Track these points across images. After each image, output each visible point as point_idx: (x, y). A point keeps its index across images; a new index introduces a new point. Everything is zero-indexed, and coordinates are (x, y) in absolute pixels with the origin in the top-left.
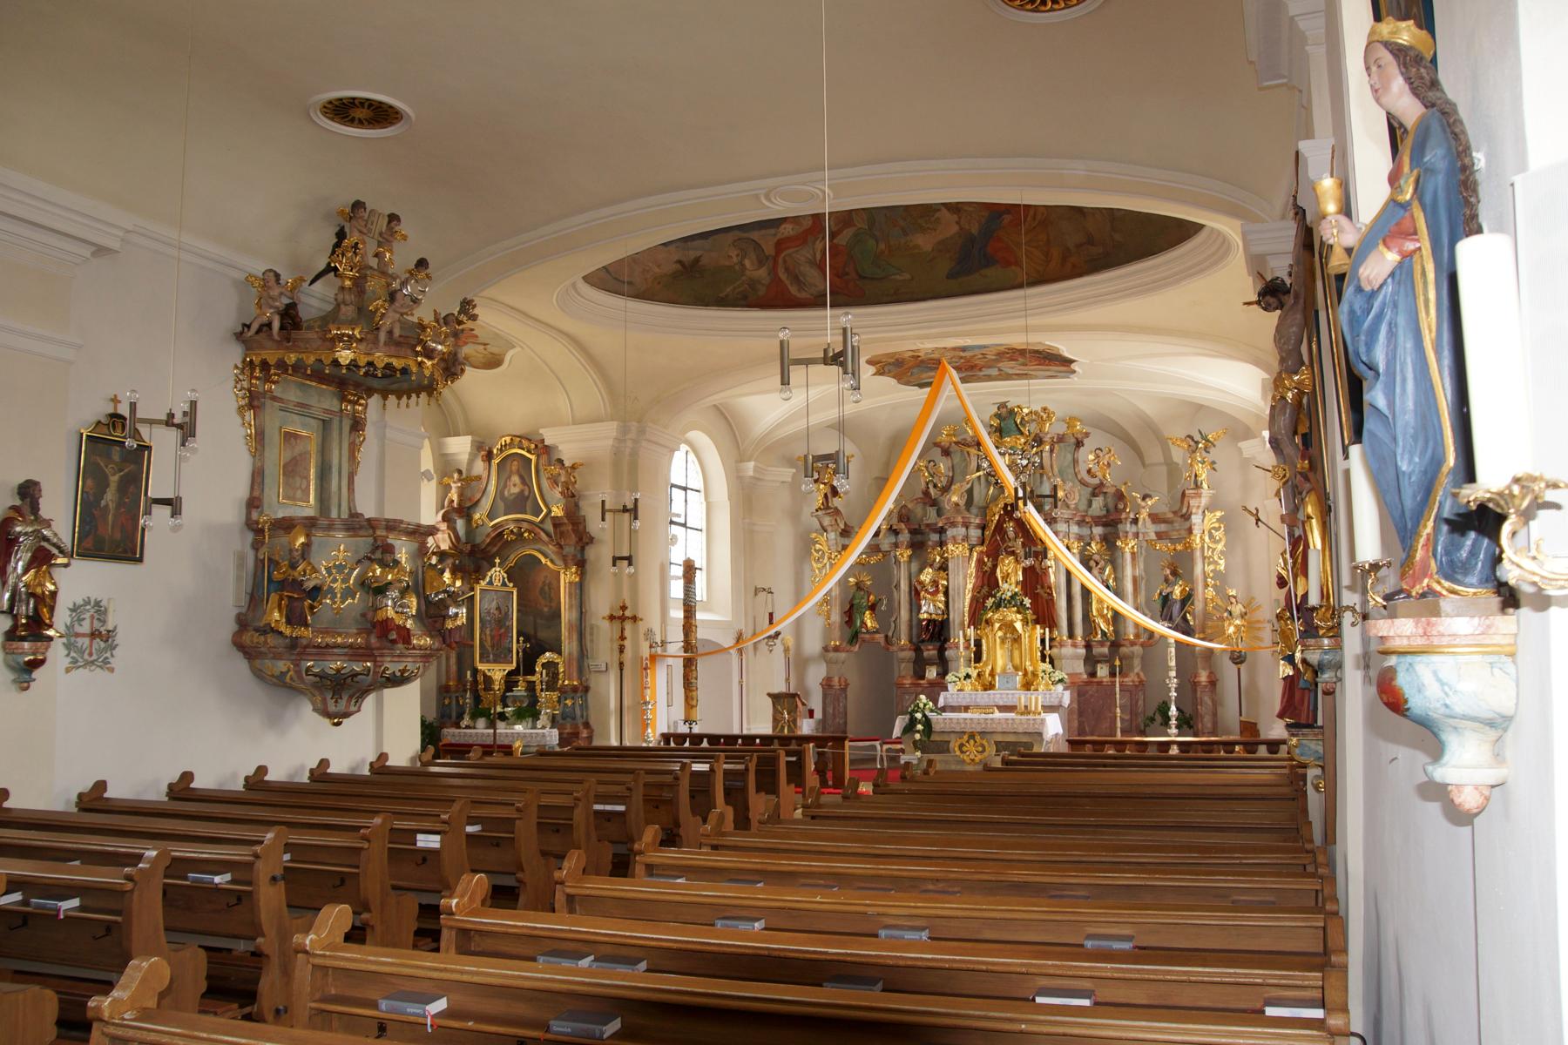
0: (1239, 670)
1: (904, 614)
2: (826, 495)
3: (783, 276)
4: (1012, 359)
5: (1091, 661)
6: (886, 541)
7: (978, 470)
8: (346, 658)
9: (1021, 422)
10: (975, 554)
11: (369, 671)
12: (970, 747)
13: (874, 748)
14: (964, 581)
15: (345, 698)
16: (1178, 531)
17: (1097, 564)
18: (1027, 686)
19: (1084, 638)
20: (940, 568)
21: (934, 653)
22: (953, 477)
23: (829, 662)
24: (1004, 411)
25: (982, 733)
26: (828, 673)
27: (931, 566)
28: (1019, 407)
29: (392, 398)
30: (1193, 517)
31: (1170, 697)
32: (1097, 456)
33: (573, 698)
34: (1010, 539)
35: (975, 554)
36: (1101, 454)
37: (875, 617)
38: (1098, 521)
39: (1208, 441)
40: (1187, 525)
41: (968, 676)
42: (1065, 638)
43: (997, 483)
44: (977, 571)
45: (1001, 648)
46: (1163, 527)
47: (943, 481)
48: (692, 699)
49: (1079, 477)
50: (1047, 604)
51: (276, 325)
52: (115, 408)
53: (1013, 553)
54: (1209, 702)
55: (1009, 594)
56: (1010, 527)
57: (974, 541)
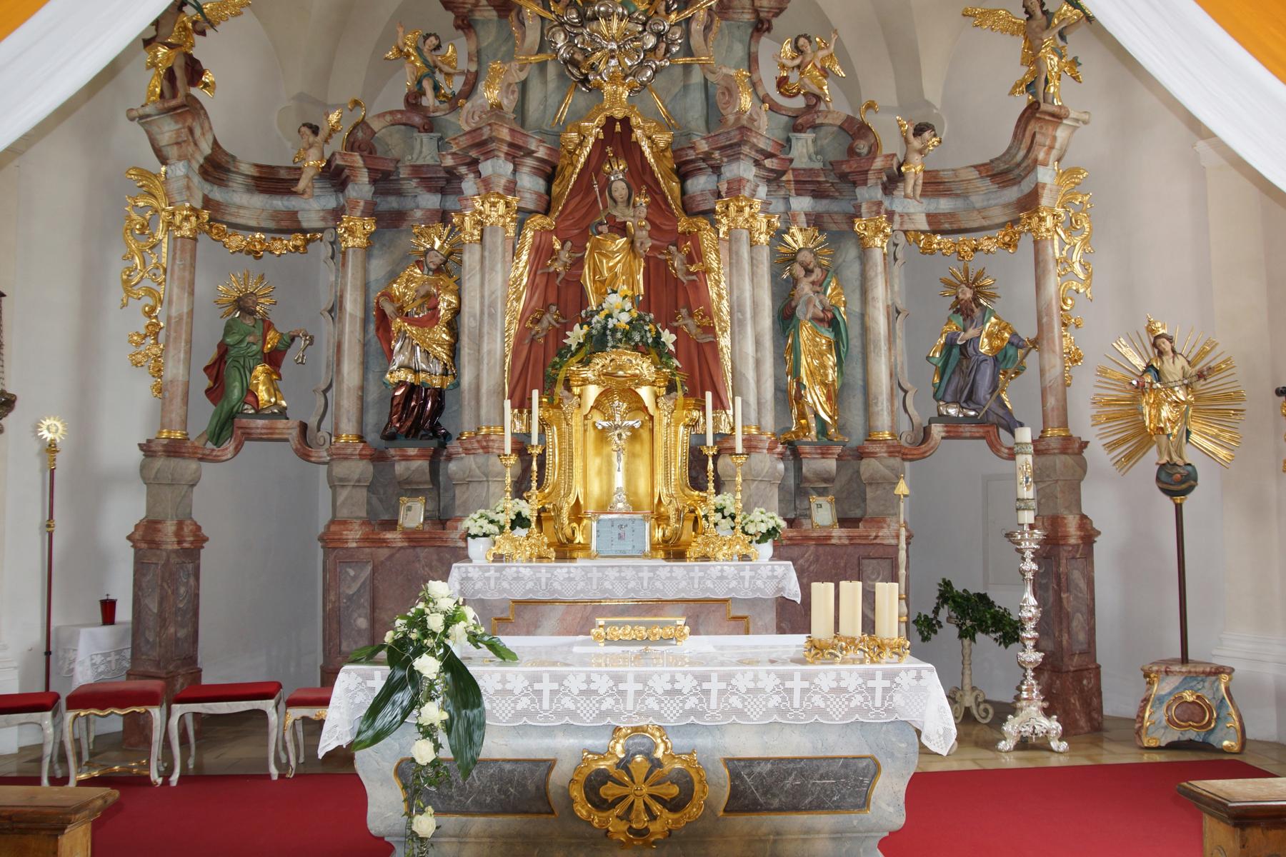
0: (1179, 509)
1: (350, 372)
2: (170, 75)
10: (530, 234)
13: (262, 714)
16: (979, 211)
17: (808, 272)
20: (438, 270)
21: (423, 464)
26: (149, 510)
27: (419, 264)
30: (1040, 169)
34: (615, 201)
35: (530, 234)
36: (809, 49)
38: (808, 185)
40: (1013, 194)
42: (754, 431)
43: (585, 81)
44: (533, 275)
45: (598, 453)
53: (622, 229)
54: (1083, 585)
55: (625, 318)
56: (617, 170)
57: (529, 202)
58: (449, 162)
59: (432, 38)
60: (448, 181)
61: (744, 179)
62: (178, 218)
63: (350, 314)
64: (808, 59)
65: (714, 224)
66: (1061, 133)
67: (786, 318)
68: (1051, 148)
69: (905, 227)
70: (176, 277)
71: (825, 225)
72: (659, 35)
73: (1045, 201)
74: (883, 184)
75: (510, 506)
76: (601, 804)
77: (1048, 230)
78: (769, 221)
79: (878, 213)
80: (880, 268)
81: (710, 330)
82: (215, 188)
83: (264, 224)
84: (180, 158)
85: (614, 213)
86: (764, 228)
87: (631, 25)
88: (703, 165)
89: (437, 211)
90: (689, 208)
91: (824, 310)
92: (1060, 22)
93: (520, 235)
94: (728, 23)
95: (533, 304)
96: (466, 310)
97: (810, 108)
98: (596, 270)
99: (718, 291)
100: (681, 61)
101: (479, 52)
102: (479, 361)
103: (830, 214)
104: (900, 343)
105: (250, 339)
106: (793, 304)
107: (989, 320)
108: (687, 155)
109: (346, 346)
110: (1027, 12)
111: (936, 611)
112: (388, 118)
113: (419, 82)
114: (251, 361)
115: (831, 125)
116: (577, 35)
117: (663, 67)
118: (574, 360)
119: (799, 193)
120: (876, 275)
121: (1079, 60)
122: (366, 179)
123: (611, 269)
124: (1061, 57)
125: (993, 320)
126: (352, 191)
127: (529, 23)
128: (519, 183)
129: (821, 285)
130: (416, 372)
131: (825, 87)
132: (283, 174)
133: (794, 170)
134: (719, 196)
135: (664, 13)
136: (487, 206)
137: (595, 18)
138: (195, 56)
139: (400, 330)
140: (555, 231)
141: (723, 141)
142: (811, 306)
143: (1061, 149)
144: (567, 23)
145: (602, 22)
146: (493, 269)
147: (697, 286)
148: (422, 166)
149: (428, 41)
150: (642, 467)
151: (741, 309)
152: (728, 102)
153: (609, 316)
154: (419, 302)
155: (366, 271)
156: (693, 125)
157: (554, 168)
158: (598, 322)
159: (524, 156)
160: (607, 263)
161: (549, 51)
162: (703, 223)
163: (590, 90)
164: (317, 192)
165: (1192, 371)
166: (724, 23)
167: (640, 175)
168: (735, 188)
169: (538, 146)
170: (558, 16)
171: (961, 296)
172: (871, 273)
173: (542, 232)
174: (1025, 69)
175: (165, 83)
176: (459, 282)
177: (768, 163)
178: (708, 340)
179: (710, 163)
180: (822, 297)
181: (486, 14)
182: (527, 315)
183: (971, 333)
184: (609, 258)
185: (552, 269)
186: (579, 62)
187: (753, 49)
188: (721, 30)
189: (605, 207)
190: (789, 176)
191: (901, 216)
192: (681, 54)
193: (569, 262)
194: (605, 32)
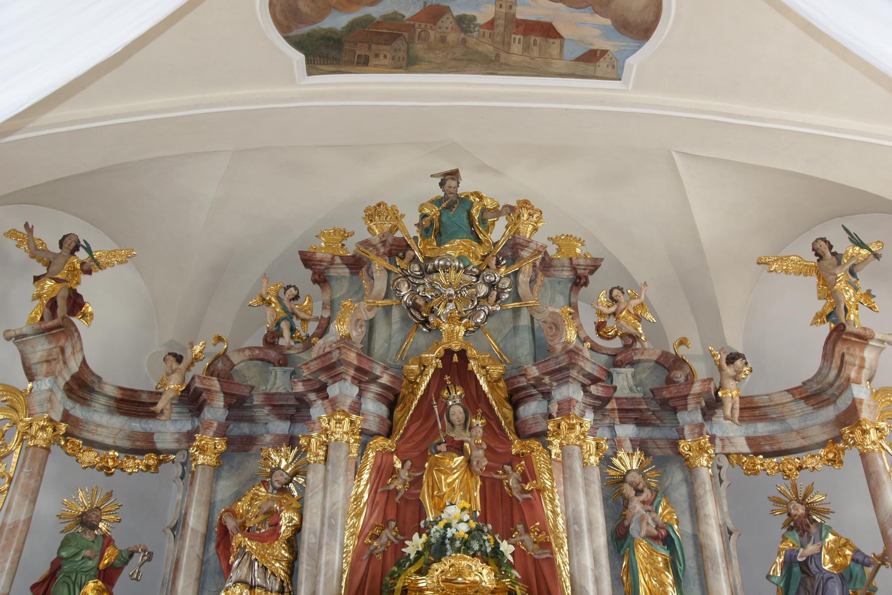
7: (387, 297)
9: (483, 221)
16: (798, 432)
17: (639, 492)
27: (264, 483)
30: (855, 387)
34: (453, 425)
36: (622, 299)
40: (829, 413)
43: (425, 322)
44: (374, 493)
46: (762, 429)
53: (458, 448)
55: (463, 528)
56: (455, 396)
58: (300, 388)
59: (292, 289)
60: (298, 410)
61: (573, 399)
62: (35, 428)
63: (192, 530)
64: (622, 306)
65: (546, 445)
66: (869, 354)
68: (861, 367)
69: (727, 450)
70: (20, 484)
71: (649, 450)
72: (492, 285)
73: (865, 414)
74: (702, 409)
77: (874, 443)
78: (597, 444)
79: (701, 434)
80: (708, 487)
81: (546, 545)
82: (78, 406)
83: (119, 443)
84: (47, 375)
85: (452, 435)
86: (593, 450)
87: (467, 277)
88: (534, 391)
89: (286, 436)
91: (657, 528)
92: (849, 261)
93: (362, 454)
94: (550, 279)
95: (372, 521)
96: (306, 526)
97: (626, 347)
98: (435, 486)
100: (511, 305)
101: (332, 302)
102: (315, 577)
103: (653, 440)
104: (735, 562)
105: (87, 553)
106: (626, 523)
107: (826, 536)
108: (519, 382)
109: (184, 560)
110: (817, 255)
112: (247, 353)
113: (278, 324)
114: (84, 577)
115: (648, 361)
116: (418, 285)
117: (495, 312)
118: (413, 570)
119: (623, 422)
120: (705, 493)
121: (872, 293)
122: (222, 404)
123: (449, 485)
124: (856, 289)
125: (831, 537)
127: (376, 275)
128: (363, 406)
129: (652, 504)
131: (640, 329)
132: (145, 398)
133: (617, 399)
134: (550, 417)
135: (494, 267)
136: (333, 423)
137: (435, 271)
138: (79, 292)
139: (239, 546)
140: (396, 452)
141: (552, 365)
142: (644, 524)
143: (871, 368)
144: (410, 276)
145: (442, 273)
146: (335, 482)
148: (275, 394)
149: (288, 292)
151: (577, 521)
152: (555, 335)
154: (261, 518)
155: (212, 492)
156: (523, 359)
157: (396, 396)
158: (437, 531)
159: (368, 382)
160: (446, 479)
161: (394, 298)
162: (535, 444)
163: (430, 330)
164: (175, 416)
166: (546, 279)
168: (566, 407)
169: (382, 373)
170: (402, 269)
171: (793, 512)
172: (700, 491)
173: (384, 455)
174: (823, 302)
175: (47, 310)
177: (593, 389)
178: (544, 556)
179: (539, 389)
180: (654, 515)
181: (340, 271)
182: (366, 531)
183: (811, 549)
184: (447, 475)
185: (392, 487)
186: (420, 306)
188: (543, 285)
189: (444, 430)
190: (612, 405)
191: (722, 440)
192: (511, 299)
193: (409, 480)
194: (444, 281)
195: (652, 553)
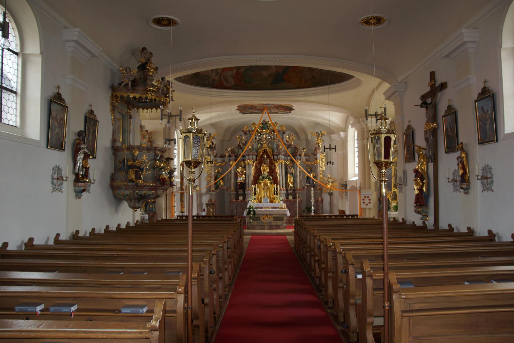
1: (233, 180)
3: (222, 79)
4: (277, 108)
5: (287, 195)
6: (227, 159)
8: (148, 190)
9: (269, 126)
11: (154, 194)
12: (266, 218)
14: (252, 170)
15: (141, 202)
17: (289, 167)
18: (271, 202)
19: (285, 188)
22: (247, 141)
23: (211, 195)
24: (264, 122)
25: (270, 215)
27: (241, 167)
28: (268, 121)
29: (141, 110)
31: (312, 205)
32: (289, 137)
33: (152, 205)
34: (265, 160)
35: (254, 164)
36: (290, 136)
37: (224, 182)
39: (322, 134)
41: (255, 199)
42: (281, 188)
44: (255, 168)
45: (263, 191)
46: (307, 157)
47: (244, 142)
48: (183, 205)
49: (284, 142)
50: (276, 178)
51: (130, 85)
52: (91, 108)
53: (266, 164)
55: (266, 175)
57: (254, 160)
67: (286, 173)
72: (270, 137)
73: (318, 159)
75: (254, 197)
76: (264, 220)
90: (274, 160)
99: (278, 170)
100: (273, 140)
101: (247, 137)
104: (301, 176)
111: (305, 209)
126: (232, 158)
130: (241, 181)
132: (223, 155)
137: (262, 135)
146: (251, 169)
147: (275, 170)
150: (268, 193)
153: (264, 175)
162: (276, 162)
165: (332, 181)
167: (268, 156)
173: (256, 163)
176: (246, 169)
187: (283, 136)
195: (290, 176)
